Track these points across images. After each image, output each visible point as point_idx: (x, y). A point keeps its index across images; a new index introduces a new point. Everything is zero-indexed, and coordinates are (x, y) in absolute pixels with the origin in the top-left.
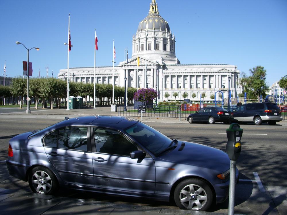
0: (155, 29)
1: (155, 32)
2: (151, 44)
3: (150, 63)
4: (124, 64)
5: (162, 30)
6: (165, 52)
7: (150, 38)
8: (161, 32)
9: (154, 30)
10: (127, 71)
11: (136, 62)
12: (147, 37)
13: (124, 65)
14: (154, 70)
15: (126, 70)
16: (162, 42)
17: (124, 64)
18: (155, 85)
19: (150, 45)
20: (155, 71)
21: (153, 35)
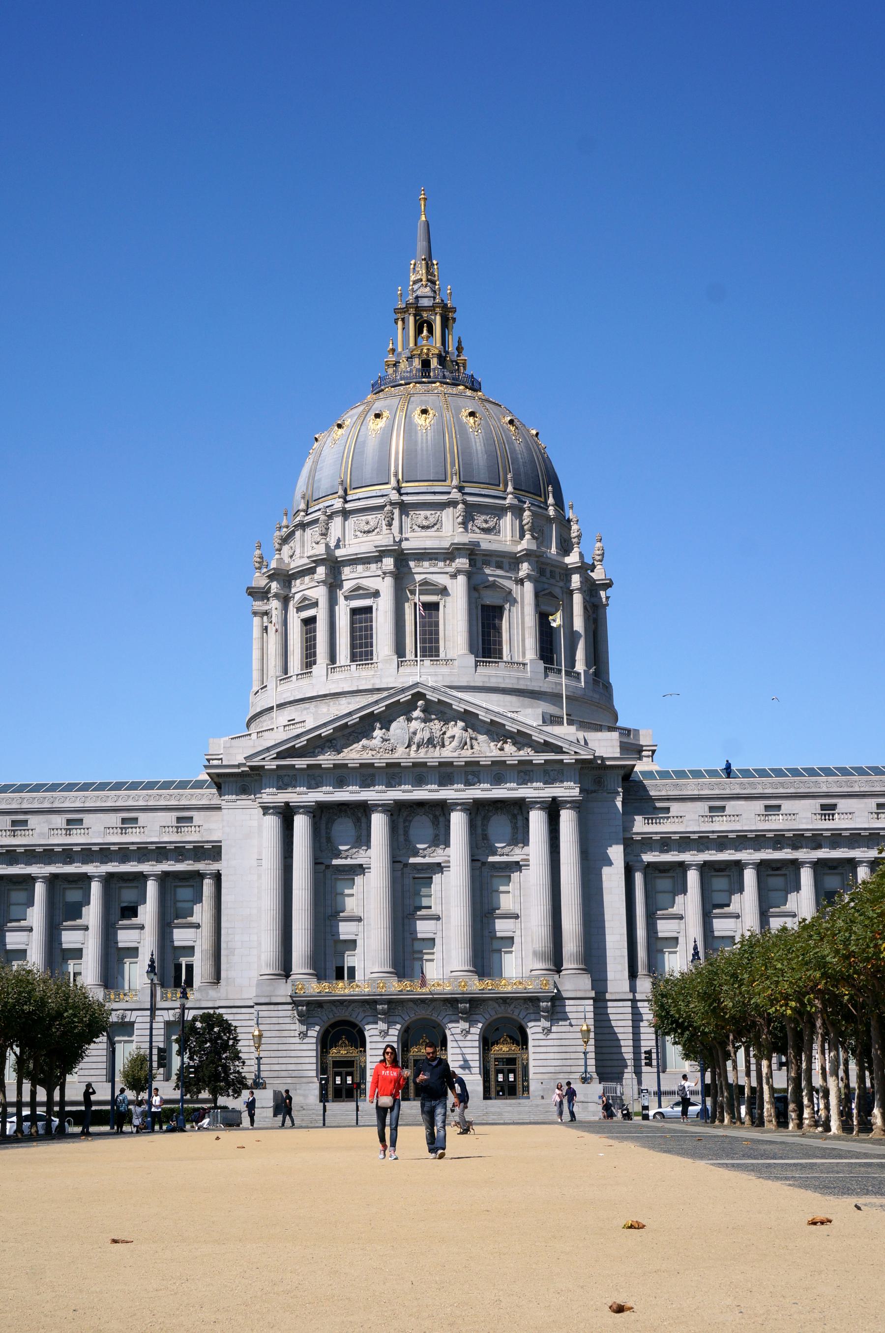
0: (407, 487)
1: (404, 508)
2: (369, 610)
3: (526, 754)
4: (280, 756)
5: (460, 489)
6: (491, 674)
7: (360, 568)
8: (453, 504)
9: (394, 496)
10: (301, 824)
11: (384, 740)
12: (338, 553)
13: (272, 765)
14: (553, 809)
15: (286, 814)
16: (458, 588)
17: (280, 756)
18: (571, 944)
19: (360, 616)
20: (567, 818)
21: (383, 539)
